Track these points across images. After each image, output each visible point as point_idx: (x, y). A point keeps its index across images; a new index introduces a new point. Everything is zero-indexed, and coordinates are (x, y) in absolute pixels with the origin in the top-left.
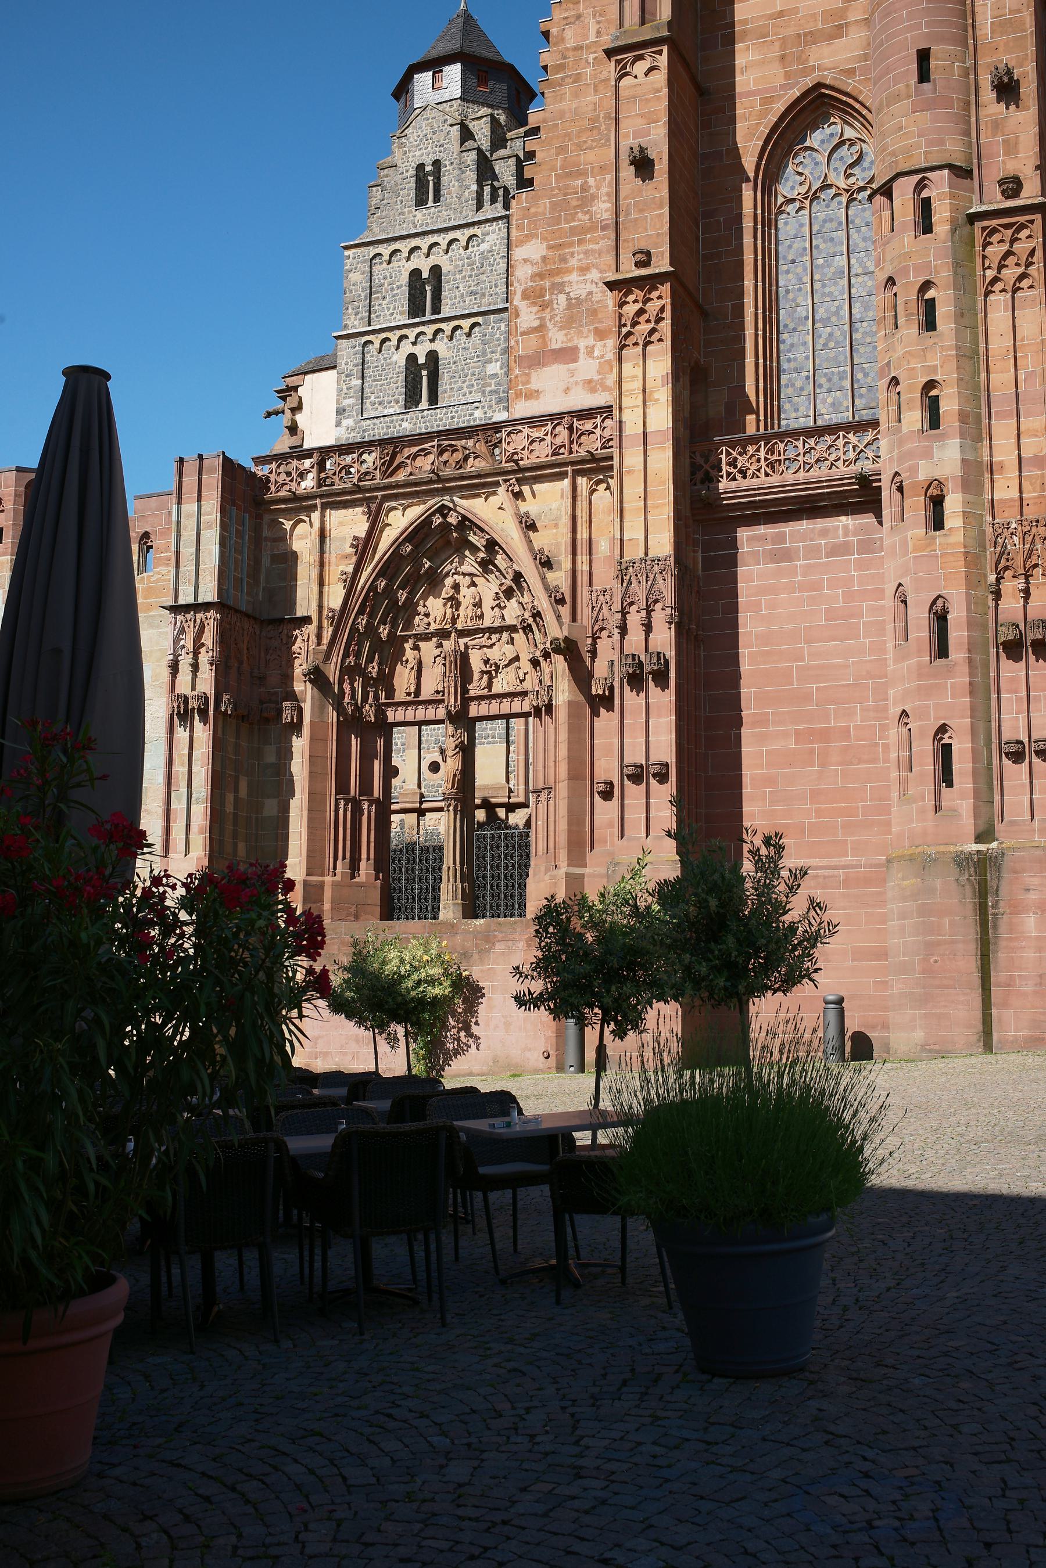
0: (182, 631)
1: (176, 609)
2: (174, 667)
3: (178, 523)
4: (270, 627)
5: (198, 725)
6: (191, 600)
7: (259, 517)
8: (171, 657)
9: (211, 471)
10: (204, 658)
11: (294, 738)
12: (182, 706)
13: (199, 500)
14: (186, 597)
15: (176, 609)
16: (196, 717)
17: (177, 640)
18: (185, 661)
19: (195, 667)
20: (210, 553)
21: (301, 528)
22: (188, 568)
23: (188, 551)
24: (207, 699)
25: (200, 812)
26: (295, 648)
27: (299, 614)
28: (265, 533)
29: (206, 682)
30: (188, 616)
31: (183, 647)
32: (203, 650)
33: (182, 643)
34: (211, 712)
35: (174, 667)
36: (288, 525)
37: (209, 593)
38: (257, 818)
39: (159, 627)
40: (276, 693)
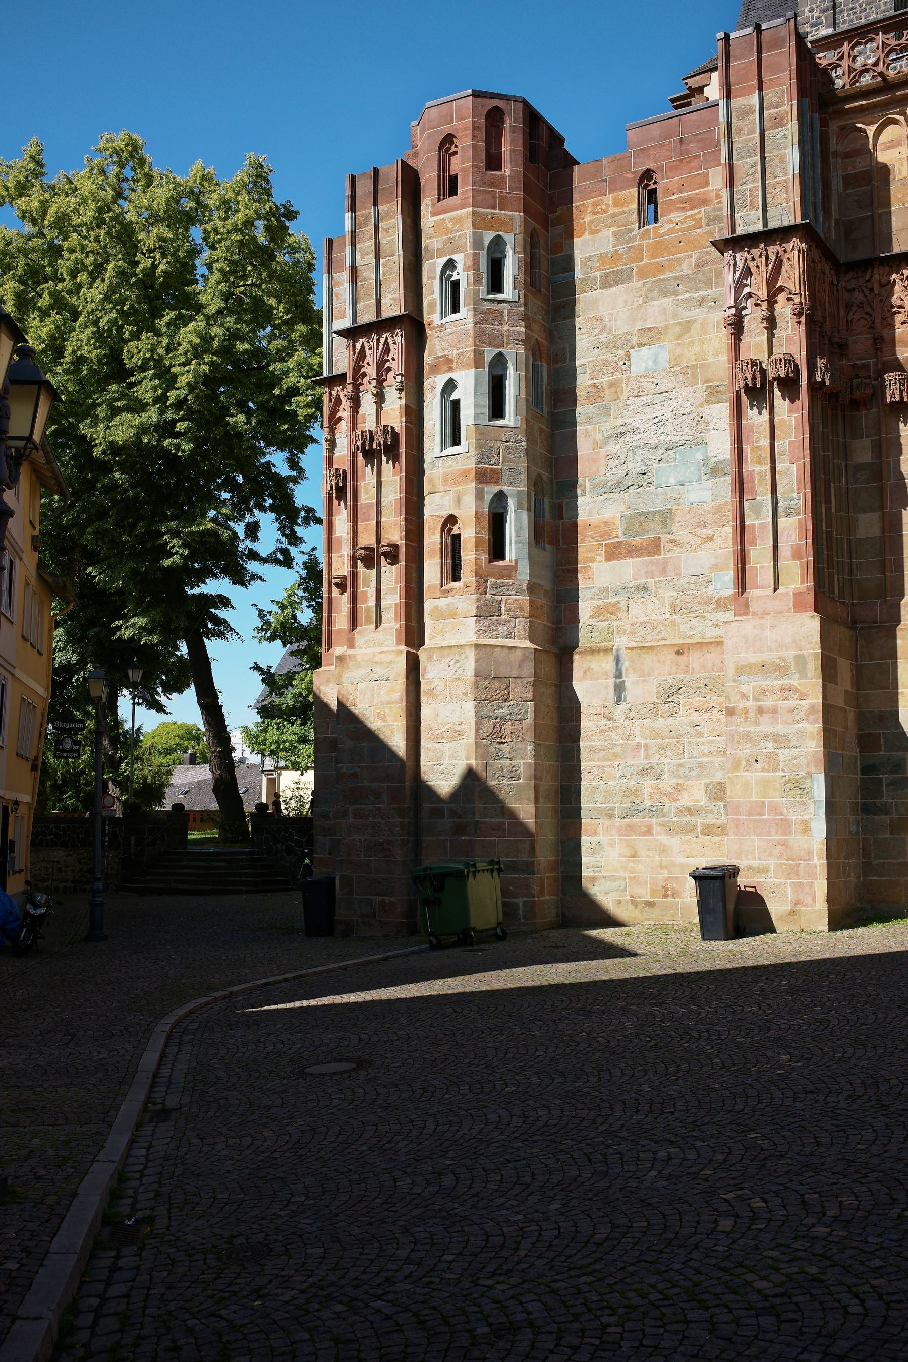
0: (747, 273)
1: (735, 243)
2: (737, 326)
3: (729, 124)
4: (850, 275)
5: (781, 404)
6: (759, 227)
7: (824, 123)
8: (733, 311)
9: (777, 44)
10: (784, 310)
11: (902, 425)
12: (758, 377)
13: (760, 88)
14: (750, 222)
15: (735, 243)
16: (777, 393)
17: (739, 287)
18: (754, 318)
19: (771, 323)
20: (783, 161)
21: (890, 132)
22: (749, 186)
23: (747, 164)
24: (796, 365)
25: (795, 529)
26: (895, 300)
27: (897, 249)
28: (833, 147)
29: (792, 339)
30: (755, 252)
31: (749, 295)
32: (782, 298)
33: (747, 290)
34: (804, 382)
35: (737, 326)
36: (871, 130)
37: (786, 210)
38: (850, 541)
39: (676, 293)
40: (866, 367)
